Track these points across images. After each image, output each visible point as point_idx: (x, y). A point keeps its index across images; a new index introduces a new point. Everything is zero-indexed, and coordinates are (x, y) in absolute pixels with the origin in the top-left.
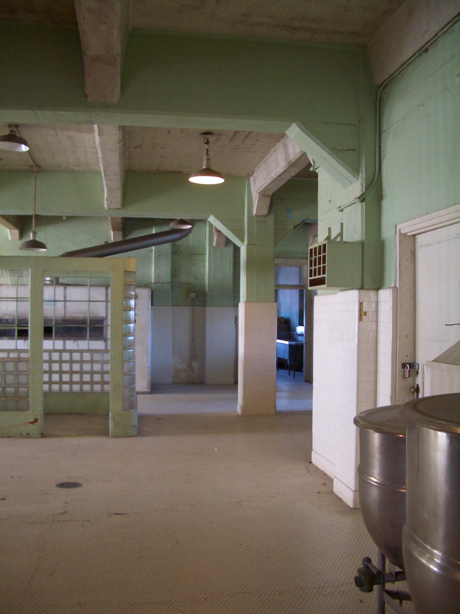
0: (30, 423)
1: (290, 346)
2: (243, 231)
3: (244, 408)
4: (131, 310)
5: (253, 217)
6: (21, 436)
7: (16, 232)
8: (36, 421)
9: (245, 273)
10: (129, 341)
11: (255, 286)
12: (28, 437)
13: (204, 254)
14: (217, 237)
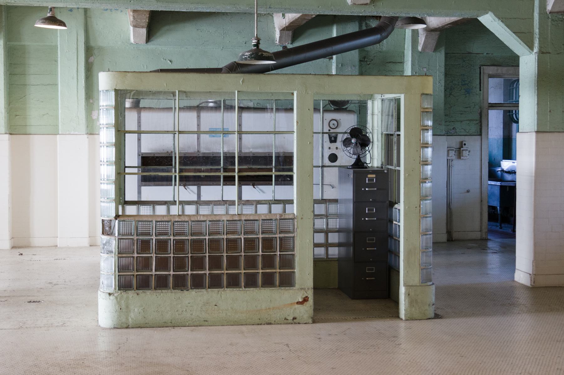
0: (298, 303)
1: (501, 187)
2: (531, 33)
3: (535, 276)
4: (427, 147)
5: (547, 14)
6: (286, 322)
7: (144, 31)
8: (305, 300)
9: (535, 92)
10: (426, 188)
11: (549, 110)
12: (295, 323)
13: (402, 63)
14: (426, 38)
